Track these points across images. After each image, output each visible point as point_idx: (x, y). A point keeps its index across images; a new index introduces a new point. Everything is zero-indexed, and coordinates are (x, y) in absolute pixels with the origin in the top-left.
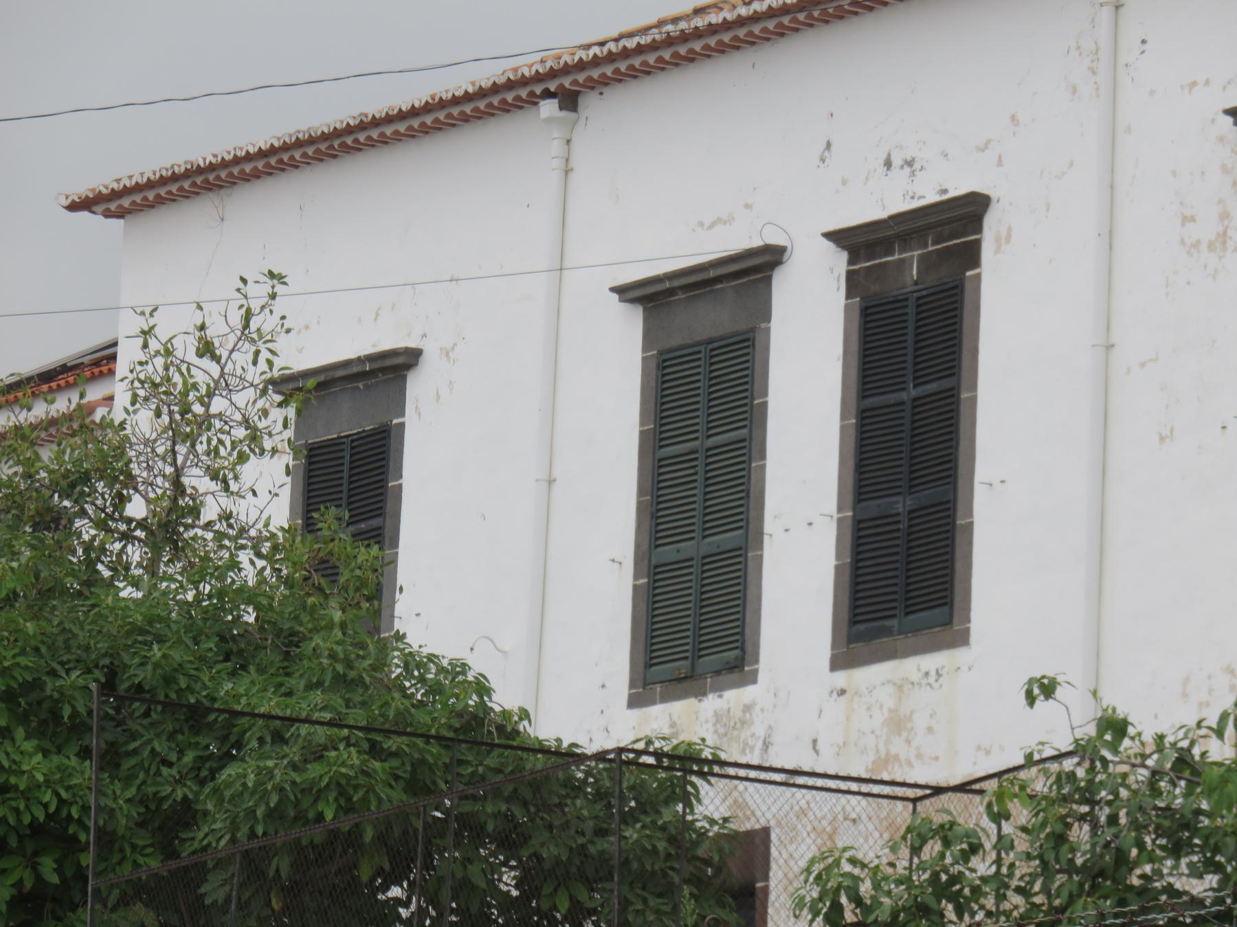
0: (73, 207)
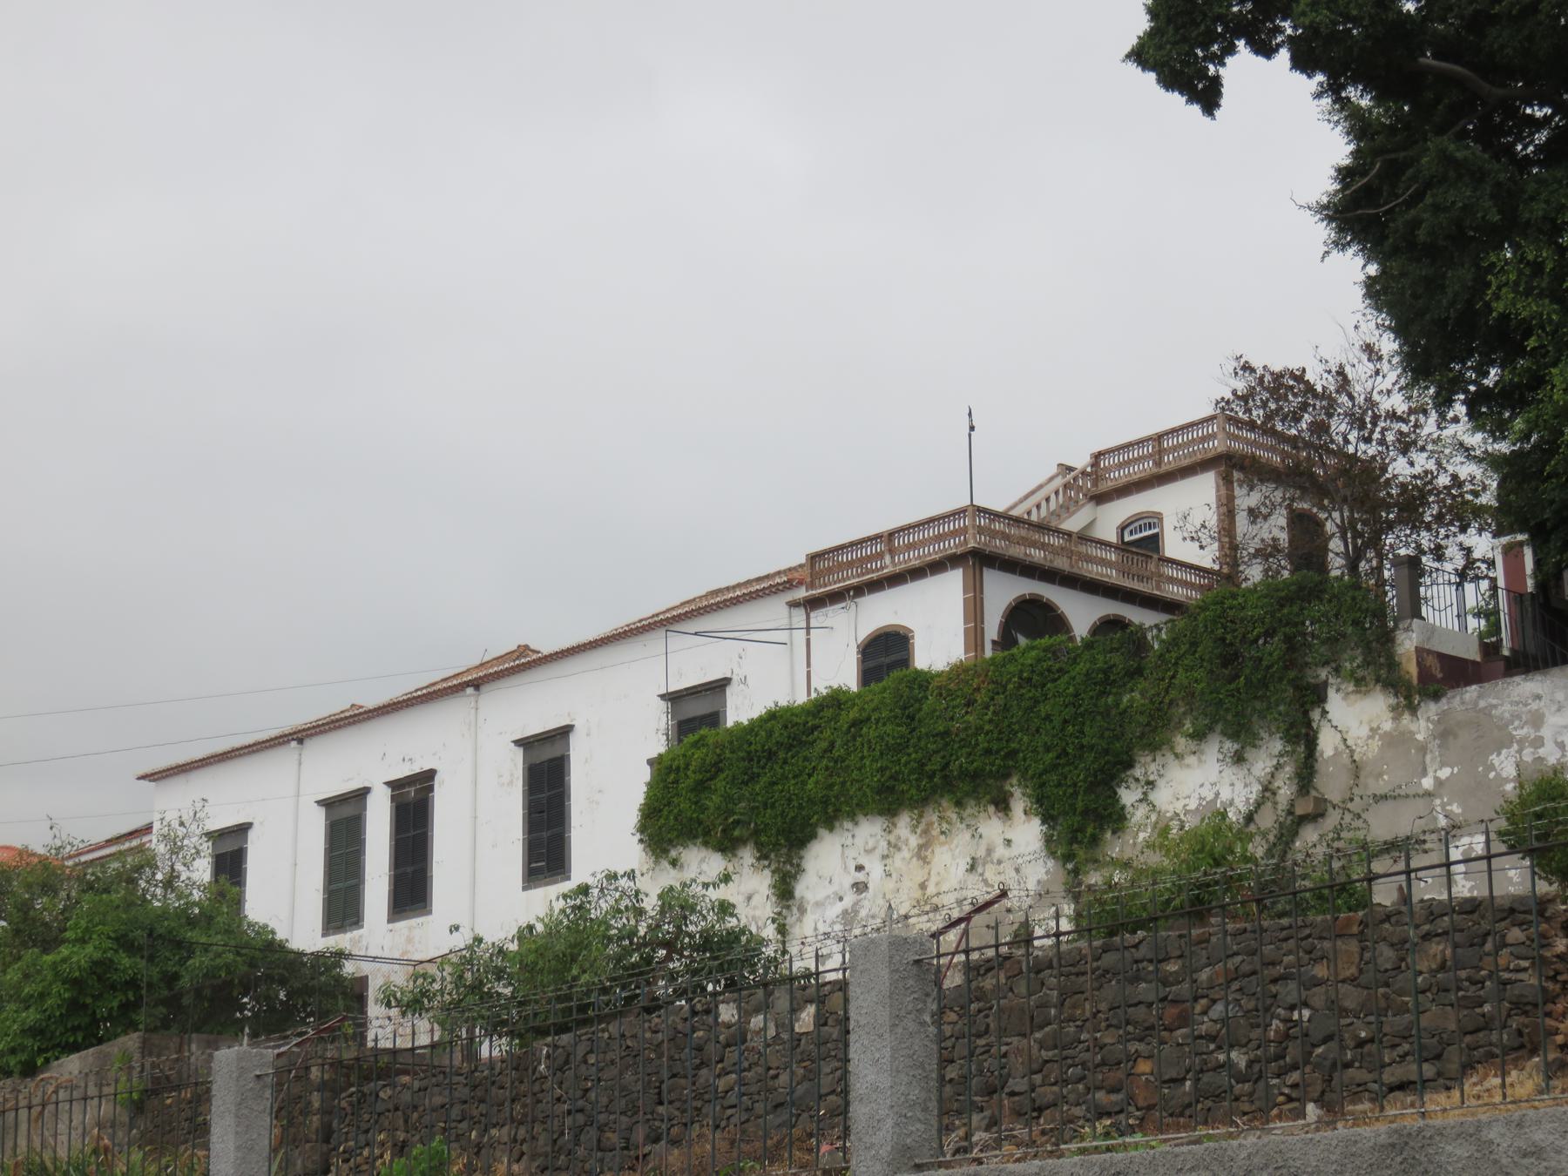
0: (139, 778)
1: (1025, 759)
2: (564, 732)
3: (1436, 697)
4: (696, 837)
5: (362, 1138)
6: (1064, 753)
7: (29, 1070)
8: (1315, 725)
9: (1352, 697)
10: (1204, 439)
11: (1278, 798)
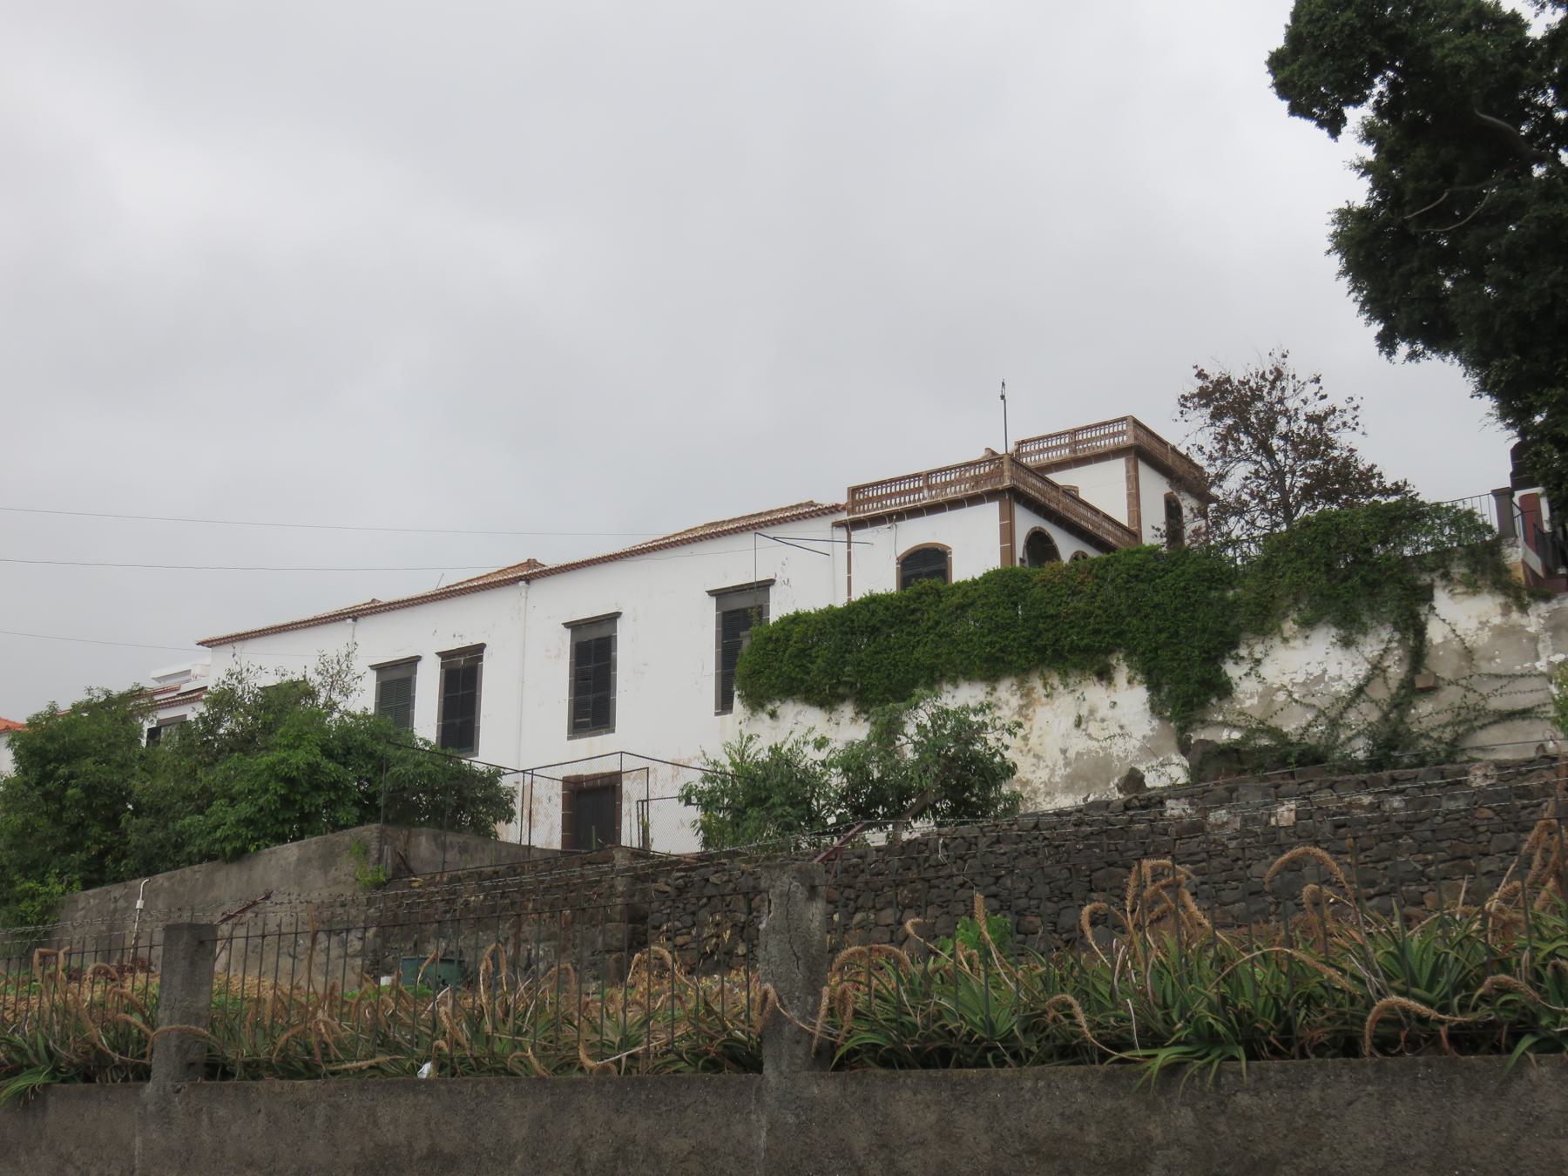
0: (202, 644)
1: (1133, 639)
2: (613, 618)
3: (1547, 598)
4: (794, 694)
5: (688, 920)
7: (239, 855)
8: (1423, 618)
10: (1114, 435)
11: (1388, 675)
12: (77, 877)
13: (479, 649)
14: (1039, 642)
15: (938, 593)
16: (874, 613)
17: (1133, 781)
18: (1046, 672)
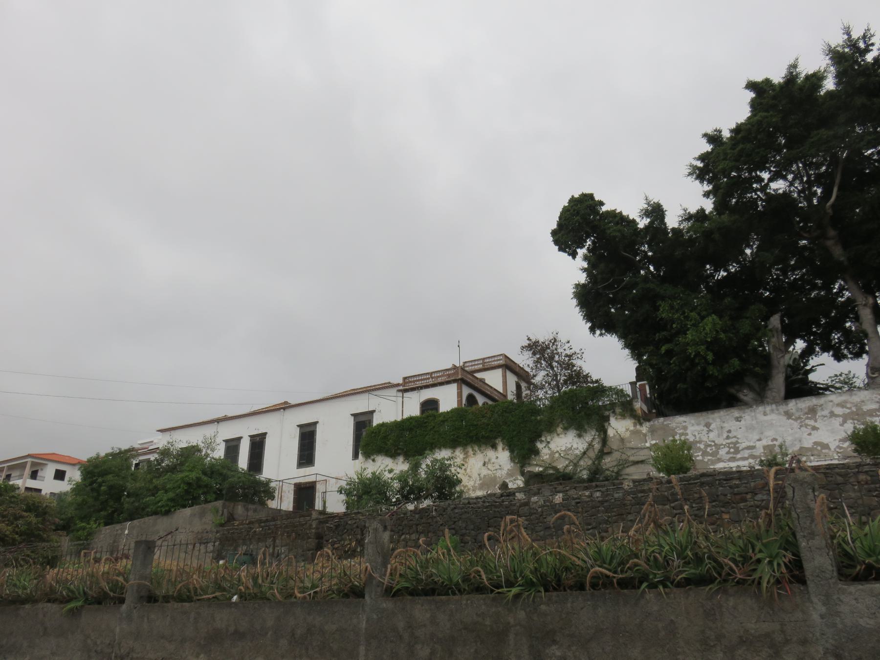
2: (315, 423)
3: (649, 420)
4: (381, 452)
5: (339, 538)
6: (520, 432)
7: (167, 513)
9: (619, 420)
10: (498, 360)
12: (102, 521)
13: (265, 434)
14: (471, 434)
15: (435, 416)
16: (411, 423)
17: (504, 485)
18: (473, 445)
